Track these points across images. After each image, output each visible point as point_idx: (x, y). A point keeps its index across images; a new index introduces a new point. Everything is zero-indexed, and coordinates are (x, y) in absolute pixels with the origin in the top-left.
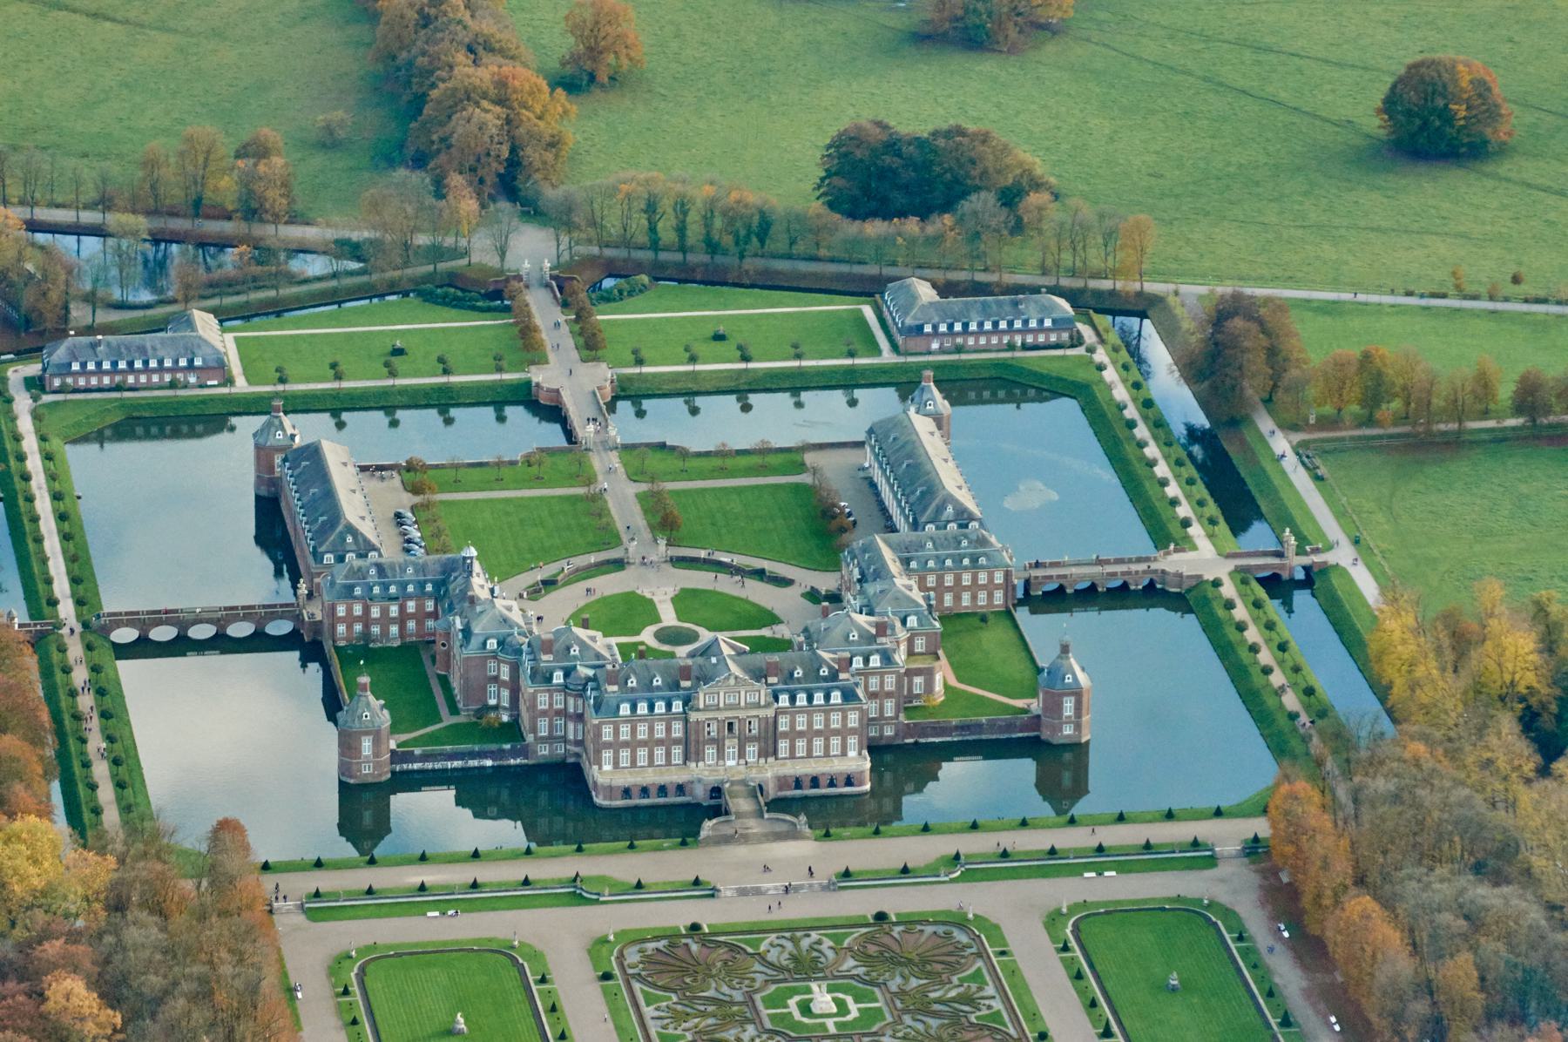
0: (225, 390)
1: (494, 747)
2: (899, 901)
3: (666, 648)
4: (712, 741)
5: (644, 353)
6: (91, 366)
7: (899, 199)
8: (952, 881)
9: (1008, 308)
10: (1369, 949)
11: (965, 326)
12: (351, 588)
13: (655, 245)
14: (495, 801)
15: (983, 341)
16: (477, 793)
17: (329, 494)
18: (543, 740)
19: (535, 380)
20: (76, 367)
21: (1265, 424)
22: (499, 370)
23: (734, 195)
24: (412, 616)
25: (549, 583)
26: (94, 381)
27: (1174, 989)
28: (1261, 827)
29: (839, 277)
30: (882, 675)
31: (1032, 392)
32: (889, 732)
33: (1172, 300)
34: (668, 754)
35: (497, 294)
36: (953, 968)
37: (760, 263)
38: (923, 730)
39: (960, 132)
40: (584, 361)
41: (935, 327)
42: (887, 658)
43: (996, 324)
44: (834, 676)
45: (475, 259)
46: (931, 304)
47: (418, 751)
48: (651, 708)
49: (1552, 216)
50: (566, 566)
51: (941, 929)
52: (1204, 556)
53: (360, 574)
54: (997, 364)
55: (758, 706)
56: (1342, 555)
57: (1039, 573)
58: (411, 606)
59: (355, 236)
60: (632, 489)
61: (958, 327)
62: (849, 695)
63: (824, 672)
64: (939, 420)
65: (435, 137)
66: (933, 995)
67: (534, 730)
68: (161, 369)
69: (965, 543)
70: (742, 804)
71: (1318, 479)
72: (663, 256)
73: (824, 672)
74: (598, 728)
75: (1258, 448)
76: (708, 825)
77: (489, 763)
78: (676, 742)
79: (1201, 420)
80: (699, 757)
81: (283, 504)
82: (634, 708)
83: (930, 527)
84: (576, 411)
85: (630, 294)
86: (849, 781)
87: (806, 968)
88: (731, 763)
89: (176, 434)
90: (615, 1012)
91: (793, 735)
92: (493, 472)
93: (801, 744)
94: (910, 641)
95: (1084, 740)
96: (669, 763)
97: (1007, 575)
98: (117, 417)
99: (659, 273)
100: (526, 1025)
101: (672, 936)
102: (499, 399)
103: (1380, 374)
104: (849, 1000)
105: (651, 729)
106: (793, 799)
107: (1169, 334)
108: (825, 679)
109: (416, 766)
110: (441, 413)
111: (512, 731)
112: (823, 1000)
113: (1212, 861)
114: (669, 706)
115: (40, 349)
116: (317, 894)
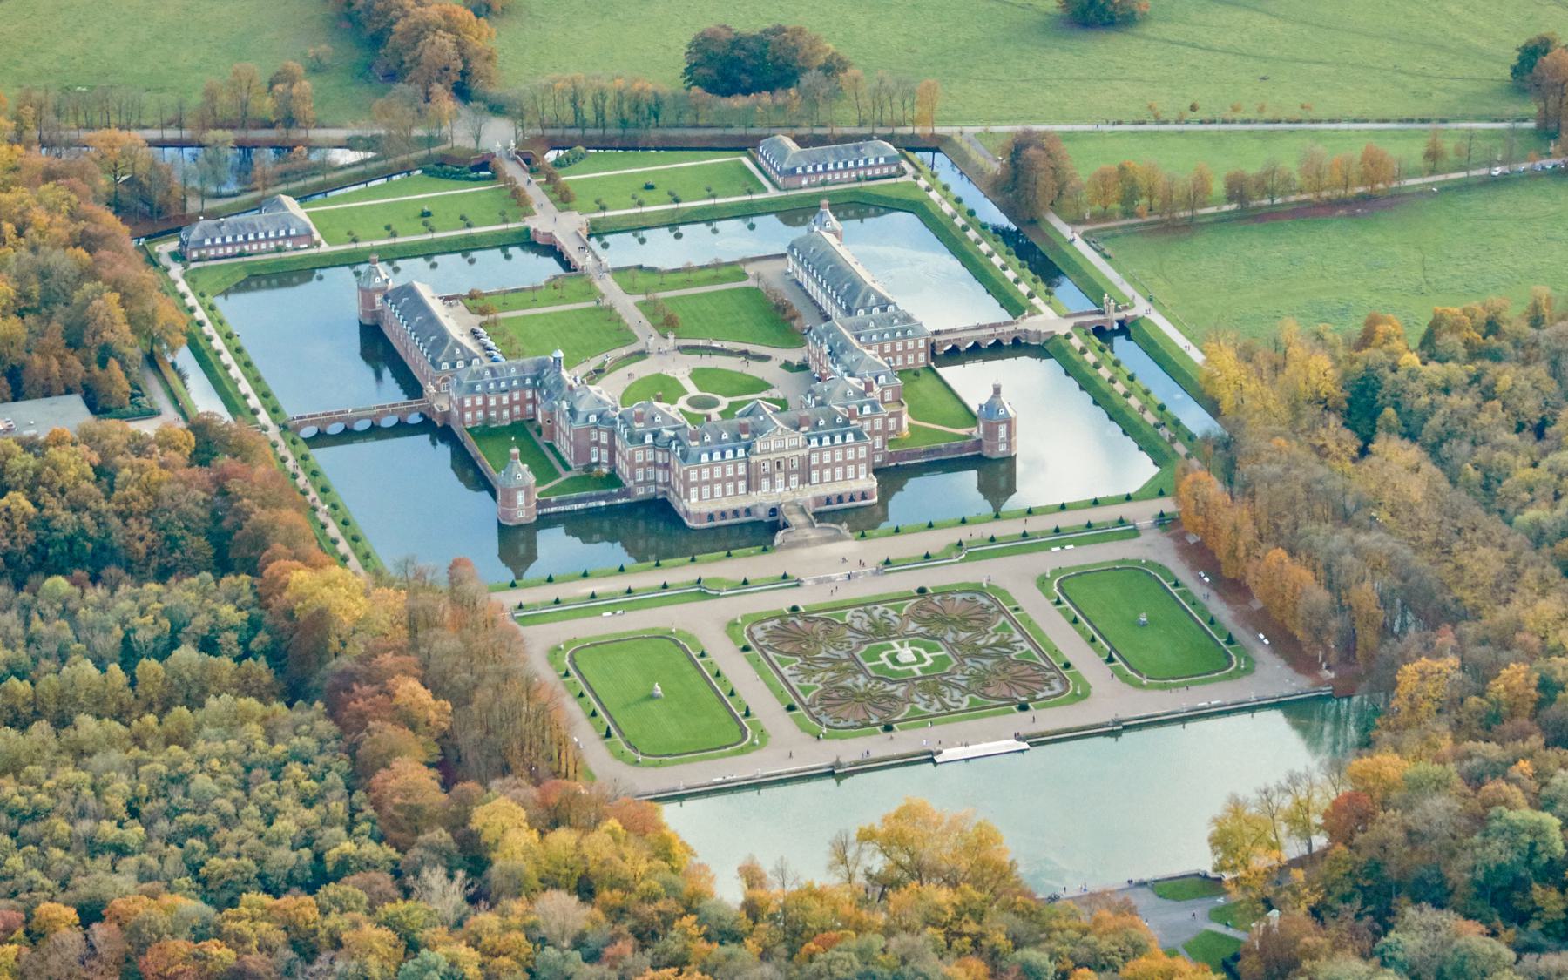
0: (314, 251)
2: (932, 578)
4: (766, 476)
5: (605, 202)
6: (218, 241)
7: (747, 80)
10: (1289, 586)
11: (825, 166)
12: (472, 387)
13: (583, 125)
14: (600, 531)
15: (837, 176)
16: (581, 524)
17: (432, 319)
18: (640, 484)
20: (208, 242)
21: (1056, 222)
22: (506, 221)
23: (637, 86)
24: (517, 403)
25: (599, 372)
26: (221, 251)
27: (1144, 625)
28: (1167, 505)
29: (714, 138)
30: (872, 419)
31: (872, 210)
32: (878, 459)
33: (957, 138)
34: (736, 488)
35: (484, 166)
36: (986, 622)
37: (660, 132)
38: (901, 456)
39: (781, 29)
40: (561, 210)
41: (804, 169)
42: (875, 408)
43: (846, 164)
44: (846, 423)
45: (456, 143)
47: (553, 499)
48: (723, 455)
49: (1193, 62)
51: (967, 596)
52: (1046, 318)
53: (478, 375)
55: (798, 448)
56: (1141, 308)
57: (938, 338)
58: (516, 396)
59: (368, 133)
60: (630, 300)
61: (820, 168)
62: (858, 435)
63: (839, 420)
64: (836, 233)
65: (406, 59)
66: (980, 643)
67: (633, 477)
70: (796, 519)
71: (1106, 257)
72: (590, 132)
73: (839, 420)
75: (1054, 236)
78: (741, 478)
79: (1003, 221)
80: (758, 488)
81: (386, 330)
82: (711, 456)
83: (861, 312)
84: (571, 249)
86: (864, 497)
87: (882, 631)
88: (780, 490)
89: (281, 285)
90: (762, 673)
91: (821, 467)
92: (529, 295)
93: (827, 472)
94: (882, 393)
97: (927, 340)
98: (242, 276)
99: (589, 143)
100: (702, 688)
101: (781, 616)
102: (503, 243)
103: (1134, 180)
104: (922, 651)
105: (724, 471)
107: (961, 162)
108: (841, 425)
109: (553, 510)
110: (465, 256)
111: (613, 479)
112: (906, 654)
113: (1136, 532)
114: (735, 453)
115: (180, 229)
116: (521, 607)
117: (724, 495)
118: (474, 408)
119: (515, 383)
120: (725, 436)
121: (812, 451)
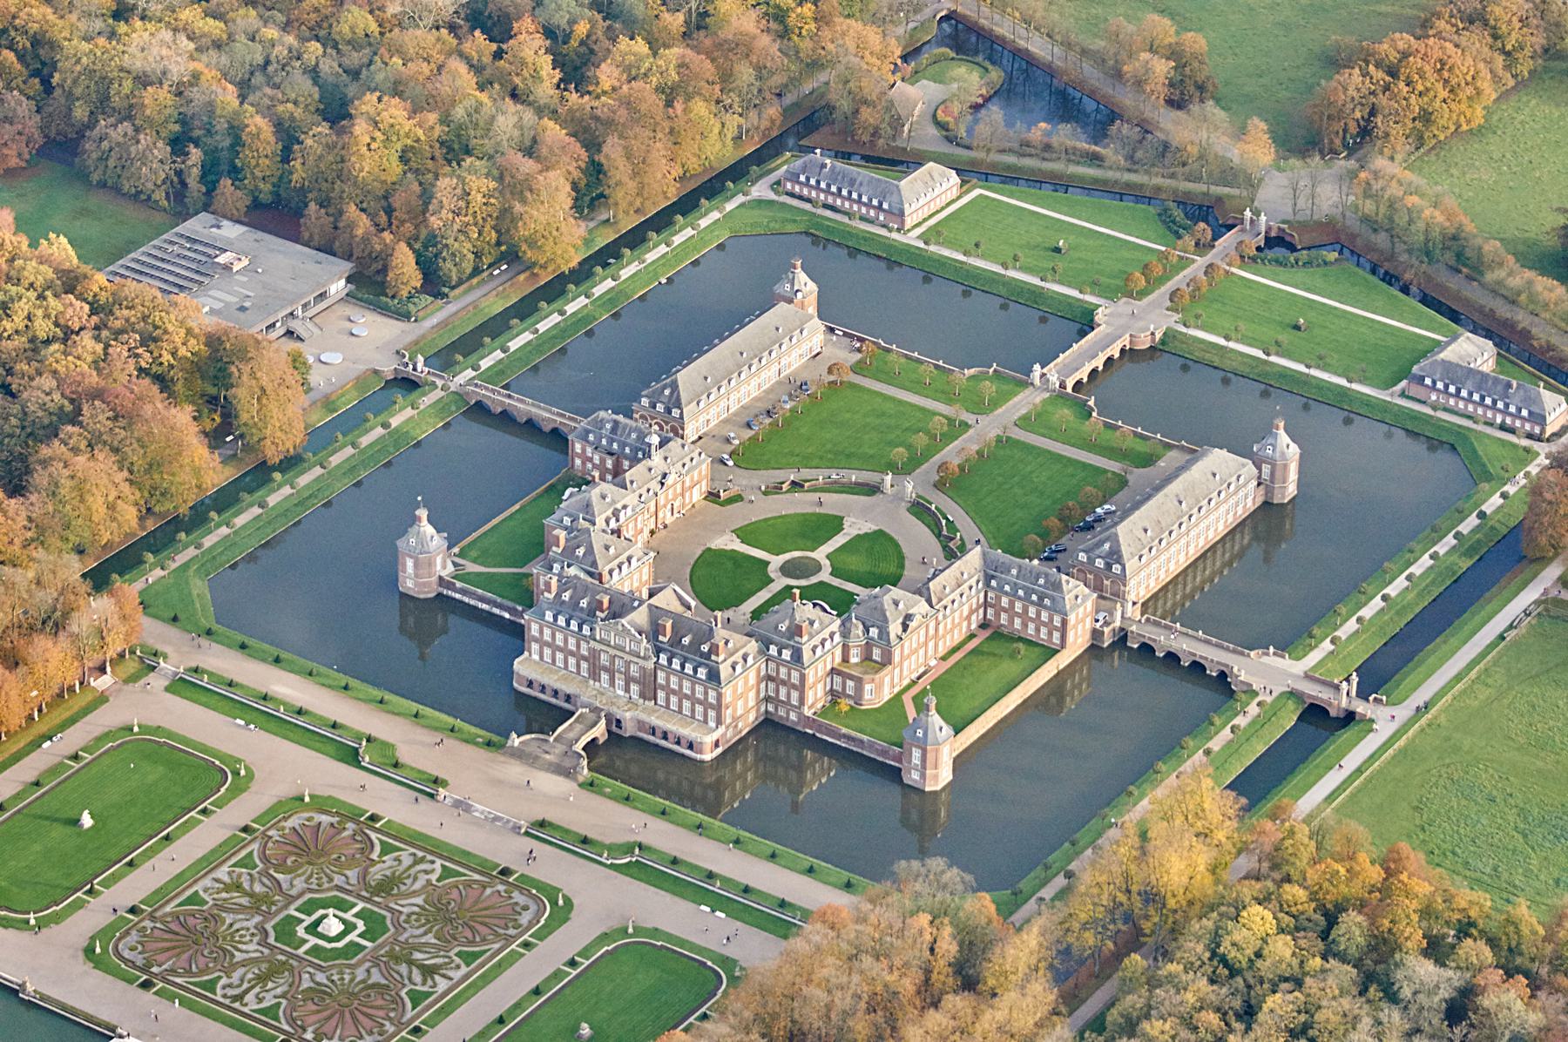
3: (772, 575)
9: (1500, 388)
11: (1458, 390)
12: (588, 432)
15: (1471, 408)
20: (802, 178)
25: (796, 485)
32: (793, 716)
34: (578, 666)
38: (820, 728)
41: (1434, 382)
43: (1483, 398)
44: (707, 656)
50: (820, 476)
53: (600, 424)
54: (1461, 432)
61: (1452, 389)
63: (705, 648)
68: (859, 201)
69: (1041, 581)
71: (1502, 637)
73: (705, 648)
74: (529, 622)
76: (515, 741)
78: (585, 659)
80: (594, 675)
86: (691, 747)
94: (868, 647)
95: (927, 789)
96: (578, 673)
106: (647, 743)
108: (702, 655)
109: (458, 596)
114: (580, 628)
116: (196, 670)
117: (566, 667)
118: (583, 455)
119: (627, 450)
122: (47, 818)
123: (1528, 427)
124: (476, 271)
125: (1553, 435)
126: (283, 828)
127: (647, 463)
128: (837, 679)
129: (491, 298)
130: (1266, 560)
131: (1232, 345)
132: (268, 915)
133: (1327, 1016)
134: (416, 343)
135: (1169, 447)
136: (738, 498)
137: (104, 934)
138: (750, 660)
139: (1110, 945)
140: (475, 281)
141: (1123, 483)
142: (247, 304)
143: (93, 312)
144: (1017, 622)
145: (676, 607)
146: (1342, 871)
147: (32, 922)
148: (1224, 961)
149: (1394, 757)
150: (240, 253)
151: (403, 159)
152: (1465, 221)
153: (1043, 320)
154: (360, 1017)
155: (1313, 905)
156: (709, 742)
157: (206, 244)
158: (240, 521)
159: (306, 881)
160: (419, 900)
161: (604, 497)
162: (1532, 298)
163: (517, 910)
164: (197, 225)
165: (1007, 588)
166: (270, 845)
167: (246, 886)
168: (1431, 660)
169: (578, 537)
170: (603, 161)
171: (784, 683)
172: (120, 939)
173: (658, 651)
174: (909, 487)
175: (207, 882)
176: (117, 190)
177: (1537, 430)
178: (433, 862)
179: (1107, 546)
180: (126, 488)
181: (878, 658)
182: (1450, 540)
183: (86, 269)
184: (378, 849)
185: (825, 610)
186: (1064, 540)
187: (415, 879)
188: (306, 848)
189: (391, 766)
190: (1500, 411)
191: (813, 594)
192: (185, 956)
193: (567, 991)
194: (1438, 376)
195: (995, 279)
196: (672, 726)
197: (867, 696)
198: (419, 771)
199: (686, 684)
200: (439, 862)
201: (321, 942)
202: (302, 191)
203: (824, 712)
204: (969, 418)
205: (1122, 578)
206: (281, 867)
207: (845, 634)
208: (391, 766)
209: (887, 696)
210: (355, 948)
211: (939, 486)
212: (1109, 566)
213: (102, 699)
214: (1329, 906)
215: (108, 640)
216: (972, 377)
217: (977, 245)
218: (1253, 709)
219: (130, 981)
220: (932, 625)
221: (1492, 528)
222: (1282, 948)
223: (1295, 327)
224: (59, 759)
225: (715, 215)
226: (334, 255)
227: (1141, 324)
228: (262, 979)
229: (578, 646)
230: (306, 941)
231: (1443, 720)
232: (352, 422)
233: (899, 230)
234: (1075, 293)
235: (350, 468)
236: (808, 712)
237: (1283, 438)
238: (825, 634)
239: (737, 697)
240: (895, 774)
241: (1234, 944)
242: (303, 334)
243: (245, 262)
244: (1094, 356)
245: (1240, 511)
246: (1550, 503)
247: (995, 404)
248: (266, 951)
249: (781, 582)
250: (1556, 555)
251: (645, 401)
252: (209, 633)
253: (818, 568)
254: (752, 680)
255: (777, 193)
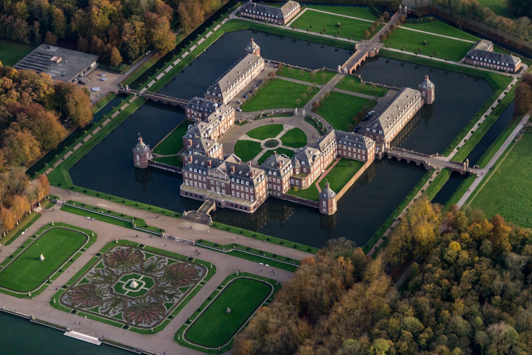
1: (175, 167)
3: (263, 147)
4: (213, 186)
8: (227, 253)
11: (483, 59)
12: (191, 105)
19: (357, 45)
20: (247, 11)
25: (265, 116)
30: (276, 178)
32: (279, 195)
41: (475, 57)
43: (492, 61)
46: (477, 50)
53: (196, 101)
54: (487, 74)
61: (481, 59)
63: (247, 174)
68: (267, 16)
69: (357, 139)
71: (514, 141)
73: (247, 174)
74: (184, 172)
77: (174, 171)
80: (210, 189)
85: (422, 22)
108: (247, 177)
109: (155, 166)
114: (202, 172)
116: (70, 202)
117: (198, 186)
118: (191, 114)
119: (206, 110)
120: (203, 164)
121: (233, 183)
122: (29, 258)
123: (509, 69)
124: (140, 54)
125: (517, 71)
126: (111, 253)
127: (215, 113)
128: (293, 180)
129: (147, 63)
130: (426, 124)
131: (403, 52)
132: (111, 283)
133: (485, 276)
134: (124, 81)
135: (389, 89)
136: (245, 122)
137: (56, 296)
138: (263, 177)
139: (403, 260)
140: (140, 57)
141: (376, 103)
142: (64, 74)
143: (14, 82)
144: (350, 154)
145: (234, 161)
146: (480, 226)
147: (30, 295)
148: (445, 261)
149: (485, 186)
150: (59, 56)
151: (110, 18)
152: (476, 2)
153: (336, 50)
154: (150, 315)
155: (472, 239)
156: (252, 206)
157: (46, 55)
158: (76, 148)
159: (122, 270)
160: (163, 272)
161: (202, 126)
162: (503, 25)
163: (197, 272)
164: (41, 48)
165: (345, 143)
166: (107, 259)
167: (102, 274)
168: (491, 152)
169: (197, 141)
170: (179, 11)
171: (275, 183)
172: (62, 297)
173: (231, 177)
174: (304, 112)
175: (88, 274)
176: (10, 39)
177: (512, 70)
178: (165, 259)
179: (376, 125)
180: (35, 141)
181: (306, 171)
182: (490, 110)
183: (8, 67)
184: (145, 256)
185: (285, 157)
186: (359, 125)
187: (160, 265)
188: (120, 258)
189: (144, 227)
190: (498, 65)
191: (280, 151)
192: (86, 300)
193: (220, 298)
194: (476, 55)
195: (318, 38)
196: (239, 202)
197: (303, 185)
198: (154, 228)
199: (242, 188)
200: (167, 259)
201: (131, 290)
202: (76, 33)
203: (289, 192)
204: (319, 86)
205: (383, 135)
206: (113, 266)
207: (294, 164)
208: (144, 227)
209: (310, 184)
210: (143, 291)
211: (313, 110)
212: (378, 132)
213: (39, 215)
214: (477, 239)
215: (39, 194)
216: (317, 72)
217: (310, 27)
218: (435, 175)
219: (68, 311)
220: (322, 158)
221: (503, 105)
222: (465, 255)
223: (424, 44)
224: (28, 238)
225: (219, 26)
226: (90, 53)
227: (371, 48)
228: (113, 305)
229: (202, 179)
230: (126, 291)
231: (499, 172)
232: (108, 110)
233: (282, 25)
234: (347, 40)
235: (110, 126)
236: (284, 192)
237: (429, 82)
238: (287, 165)
239: (260, 190)
240: (317, 211)
241: (448, 255)
242: (85, 82)
243: (61, 59)
244: (358, 61)
245: (417, 108)
246: (523, 94)
247: (327, 80)
248: (113, 296)
249: (266, 149)
250: (527, 112)
251: (208, 93)
252: (72, 188)
253: (277, 143)
254: (264, 184)
255: (239, 16)
